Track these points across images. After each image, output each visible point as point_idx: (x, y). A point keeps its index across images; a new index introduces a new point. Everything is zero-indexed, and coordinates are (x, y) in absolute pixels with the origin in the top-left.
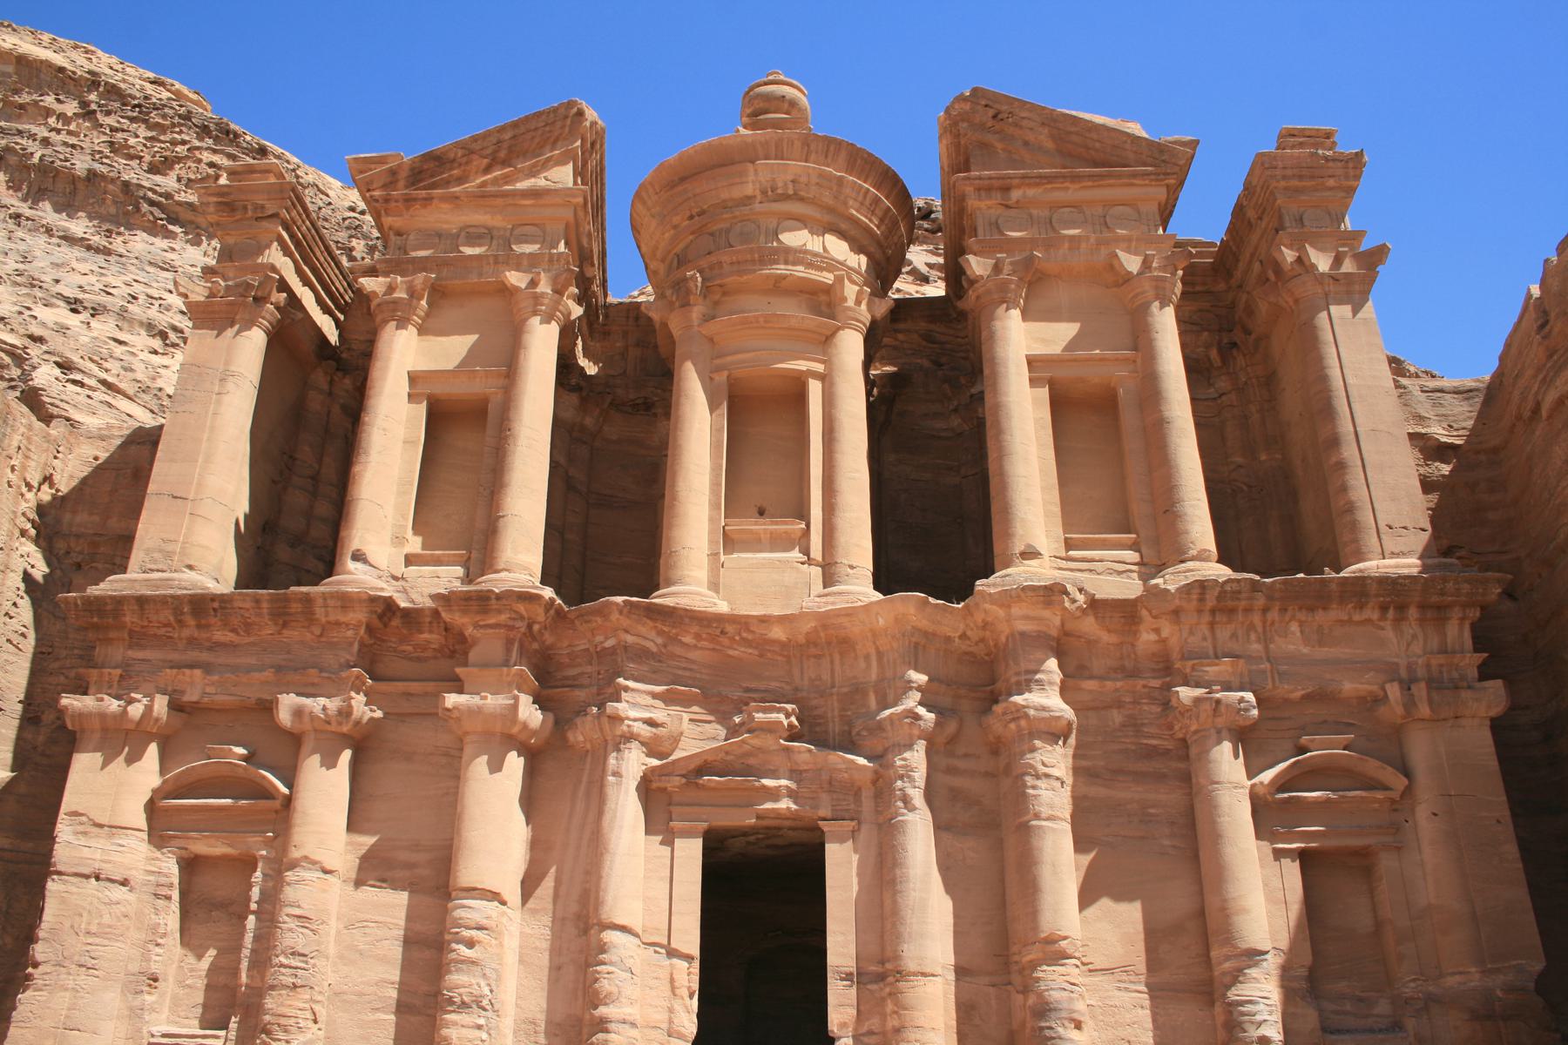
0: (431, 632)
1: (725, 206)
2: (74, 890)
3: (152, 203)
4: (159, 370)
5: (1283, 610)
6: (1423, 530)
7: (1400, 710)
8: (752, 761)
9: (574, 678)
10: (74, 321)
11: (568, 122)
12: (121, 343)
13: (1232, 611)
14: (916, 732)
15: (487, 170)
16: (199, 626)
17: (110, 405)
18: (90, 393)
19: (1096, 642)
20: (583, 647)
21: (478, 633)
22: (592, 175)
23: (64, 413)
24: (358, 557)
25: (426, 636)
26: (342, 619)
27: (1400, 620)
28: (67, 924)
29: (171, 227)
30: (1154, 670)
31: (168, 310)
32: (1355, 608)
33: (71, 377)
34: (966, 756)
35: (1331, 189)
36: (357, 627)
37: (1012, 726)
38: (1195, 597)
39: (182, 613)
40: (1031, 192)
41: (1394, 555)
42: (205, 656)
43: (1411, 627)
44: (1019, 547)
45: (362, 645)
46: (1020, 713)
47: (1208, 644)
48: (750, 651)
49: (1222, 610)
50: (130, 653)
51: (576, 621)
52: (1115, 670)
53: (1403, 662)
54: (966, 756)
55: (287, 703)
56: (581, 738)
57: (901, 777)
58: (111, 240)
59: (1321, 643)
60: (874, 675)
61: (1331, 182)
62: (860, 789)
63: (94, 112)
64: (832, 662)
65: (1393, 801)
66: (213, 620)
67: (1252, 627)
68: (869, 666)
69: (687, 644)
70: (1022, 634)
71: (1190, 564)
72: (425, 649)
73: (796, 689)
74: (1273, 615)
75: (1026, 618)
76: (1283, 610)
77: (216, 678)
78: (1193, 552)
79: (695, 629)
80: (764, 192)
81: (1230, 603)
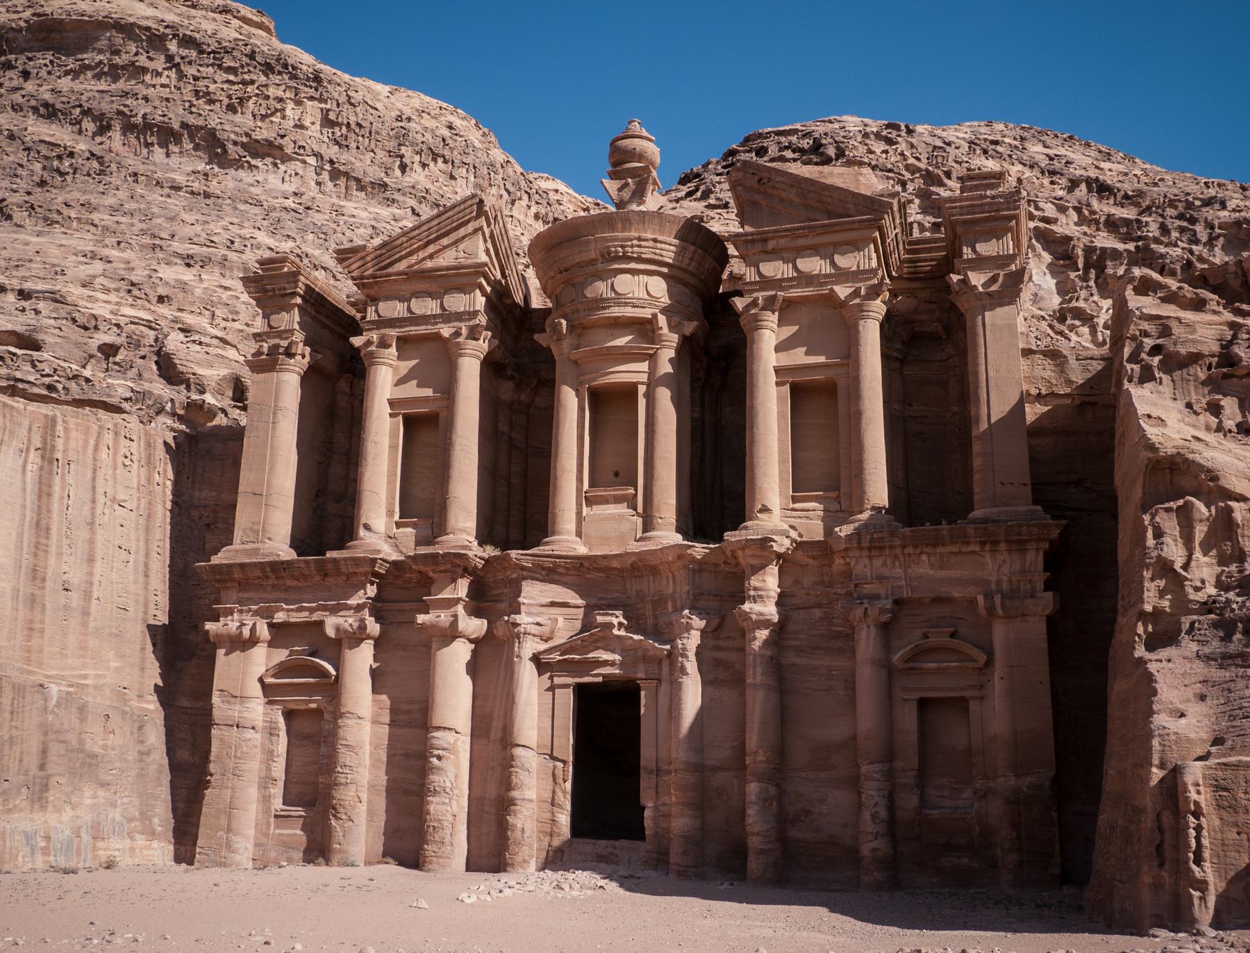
1: (580, 265)
3: (235, 143)
6: (1025, 485)
9: (498, 595)
10: (188, 275)
12: (226, 288)
16: (277, 578)
17: (223, 357)
18: (206, 349)
19: (807, 565)
23: (191, 371)
26: (356, 570)
27: (993, 552)
28: (225, 753)
29: (253, 162)
33: (192, 338)
34: (727, 638)
37: (745, 624)
40: (782, 242)
42: (282, 595)
46: (746, 616)
49: (876, 548)
52: (818, 583)
53: (994, 579)
58: (209, 183)
59: (941, 568)
63: (179, 64)
65: (981, 669)
68: (668, 584)
69: (561, 574)
70: (752, 566)
72: (409, 582)
74: (910, 550)
75: (753, 556)
80: (603, 256)
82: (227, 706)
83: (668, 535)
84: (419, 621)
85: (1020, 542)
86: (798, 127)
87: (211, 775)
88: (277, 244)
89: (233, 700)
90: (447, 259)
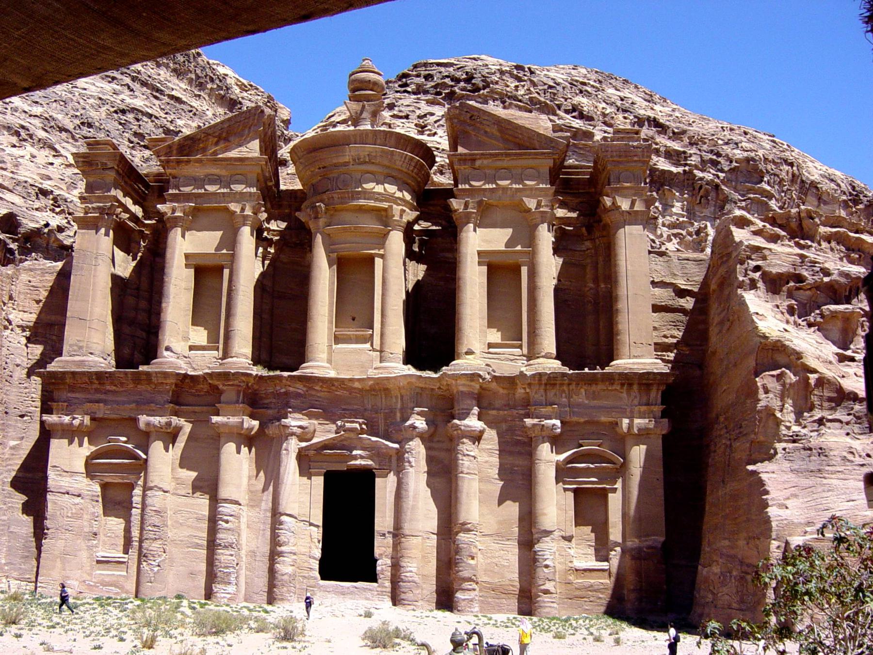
1: (336, 166)
2: (58, 498)
4: (19, 160)
5: (578, 384)
8: (345, 443)
9: (267, 404)
11: (256, 117)
13: (555, 384)
14: (414, 433)
15: (217, 144)
16: (100, 384)
21: (225, 388)
22: (270, 147)
24: (168, 349)
28: (58, 513)
31: (16, 111)
34: (438, 441)
35: (636, 161)
36: (172, 384)
37: (455, 432)
40: (485, 162)
41: (635, 357)
42: (103, 397)
44: (465, 350)
45: (173, 391)
50: (69, 395)
52: (505, 406)
54: (438, 441)
55: (143, 419)
56: (271, 432)
57: (408, 452)
59: (594, 399)
60: (399, 406)
61: (636, 158)
62: (391, 456)
65: (617, 469)
67: (564, 391)
68: (397, 402)
70: (462, 392)
71: (541, 360)
74: (573, 386)
76: (578, 384)
77: (109, 407)
78: (543, 354)
80: (354, 160)
82: (60, 478)
84: (213, 421)
86: (452, 61)
87: (48, 529)
88: (30, 109)
89: (65, 474)
90: (233, 154)
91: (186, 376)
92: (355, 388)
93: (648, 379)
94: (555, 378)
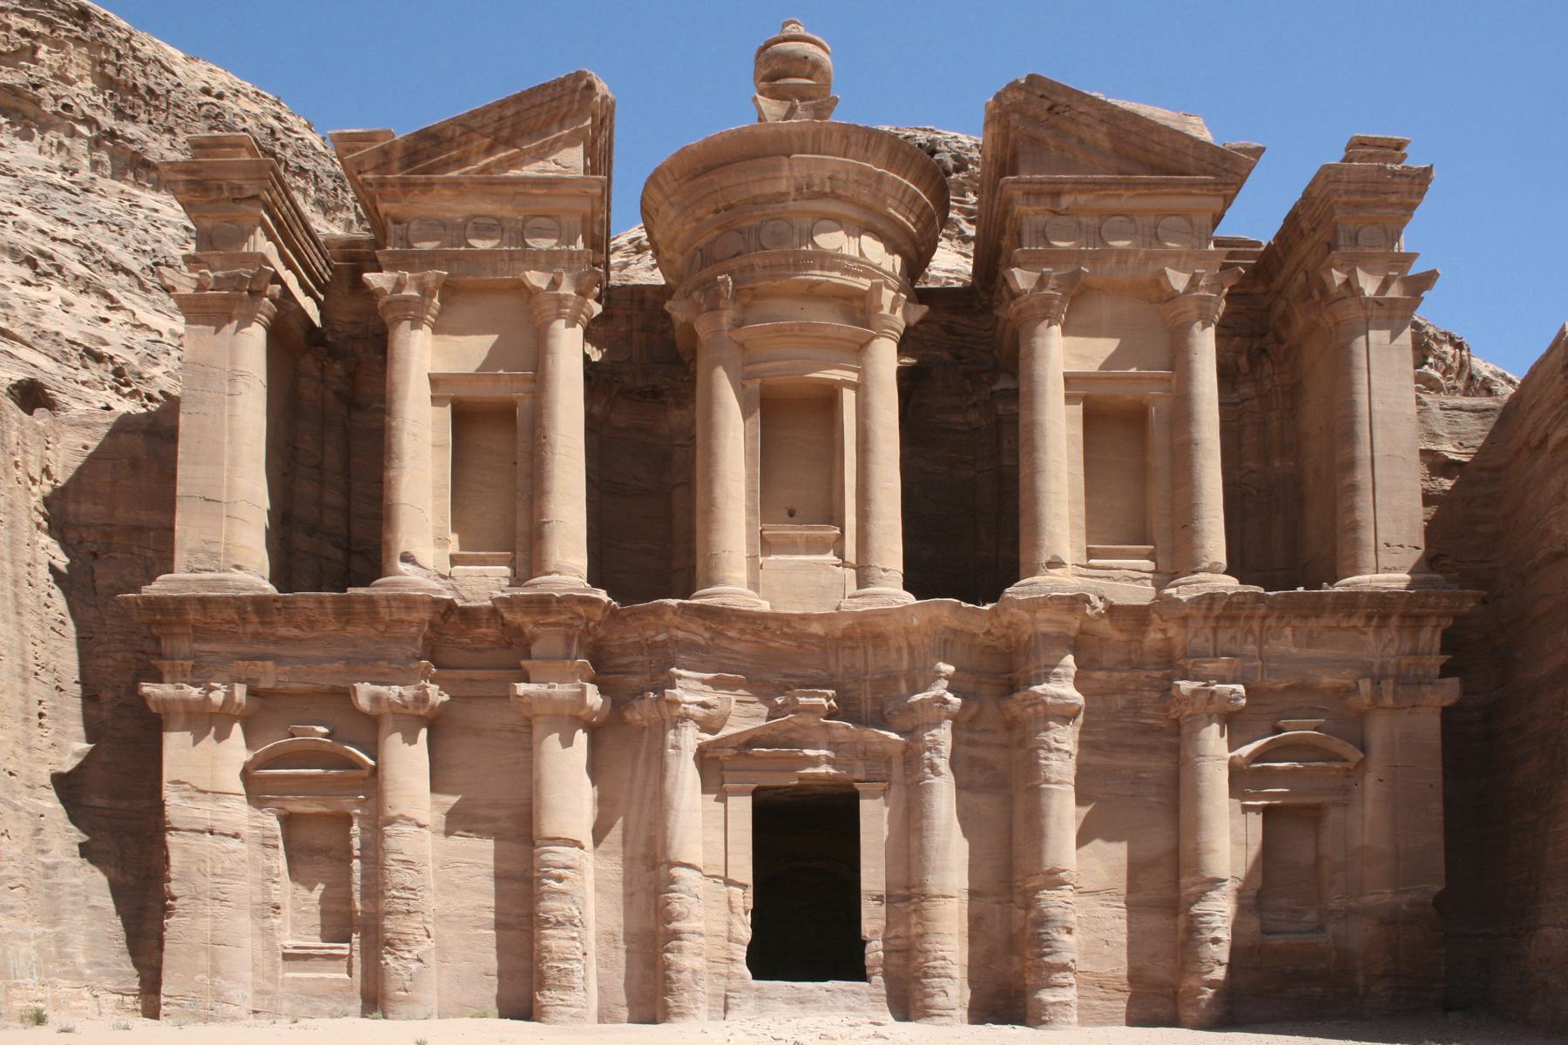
0: (489, 627)
5: (1281, 618)
7: (1367, 701)
9: (626, 666)
13: (1234, 618)
16: (262, 623)
19: (1108, 639)
20: (634, 640)
25: (484, 630)
26: (405, 617)
30: (1157, 663)
32: (1344, 617)
36: (422, 622)
38: (1203, 606)
39: (245, 612)
43: (1390, 633)
45: (425, 639)
47: (1210, 646)
48: (790, 643)
49: (1226, 617)
50: (196, 646)
51: (628, 619)
59: (1309, 645)
64: (866, 654)
66: (276, 618)
67: (1250, 631)
68: (901, 658)
69: (730, 638)
70: (1045, 635)
73: (832, 675)
74: (1271, 622)
75: (1049, 621)
76: (1281, 618)
79: (741, 625)
81: (1234, 612)
83: (891, 591)
85: (1418, 617)
91: (450, 605)
92: (811, 636)
93: (1423, 606)
94: (1241, 605)
